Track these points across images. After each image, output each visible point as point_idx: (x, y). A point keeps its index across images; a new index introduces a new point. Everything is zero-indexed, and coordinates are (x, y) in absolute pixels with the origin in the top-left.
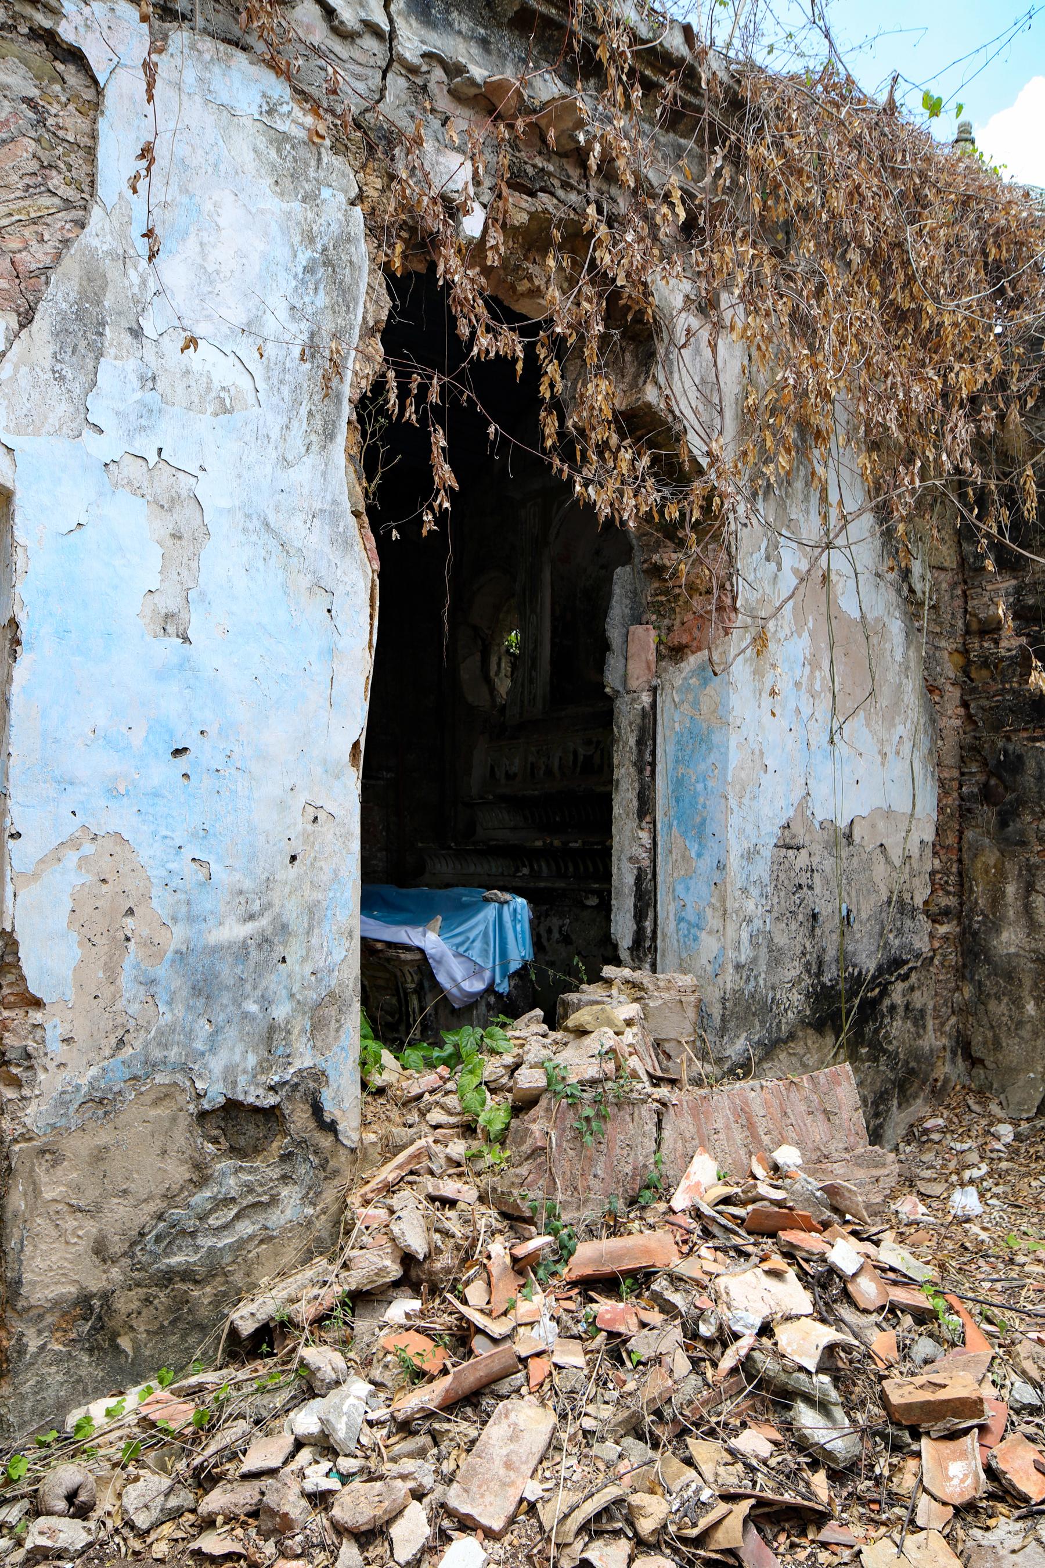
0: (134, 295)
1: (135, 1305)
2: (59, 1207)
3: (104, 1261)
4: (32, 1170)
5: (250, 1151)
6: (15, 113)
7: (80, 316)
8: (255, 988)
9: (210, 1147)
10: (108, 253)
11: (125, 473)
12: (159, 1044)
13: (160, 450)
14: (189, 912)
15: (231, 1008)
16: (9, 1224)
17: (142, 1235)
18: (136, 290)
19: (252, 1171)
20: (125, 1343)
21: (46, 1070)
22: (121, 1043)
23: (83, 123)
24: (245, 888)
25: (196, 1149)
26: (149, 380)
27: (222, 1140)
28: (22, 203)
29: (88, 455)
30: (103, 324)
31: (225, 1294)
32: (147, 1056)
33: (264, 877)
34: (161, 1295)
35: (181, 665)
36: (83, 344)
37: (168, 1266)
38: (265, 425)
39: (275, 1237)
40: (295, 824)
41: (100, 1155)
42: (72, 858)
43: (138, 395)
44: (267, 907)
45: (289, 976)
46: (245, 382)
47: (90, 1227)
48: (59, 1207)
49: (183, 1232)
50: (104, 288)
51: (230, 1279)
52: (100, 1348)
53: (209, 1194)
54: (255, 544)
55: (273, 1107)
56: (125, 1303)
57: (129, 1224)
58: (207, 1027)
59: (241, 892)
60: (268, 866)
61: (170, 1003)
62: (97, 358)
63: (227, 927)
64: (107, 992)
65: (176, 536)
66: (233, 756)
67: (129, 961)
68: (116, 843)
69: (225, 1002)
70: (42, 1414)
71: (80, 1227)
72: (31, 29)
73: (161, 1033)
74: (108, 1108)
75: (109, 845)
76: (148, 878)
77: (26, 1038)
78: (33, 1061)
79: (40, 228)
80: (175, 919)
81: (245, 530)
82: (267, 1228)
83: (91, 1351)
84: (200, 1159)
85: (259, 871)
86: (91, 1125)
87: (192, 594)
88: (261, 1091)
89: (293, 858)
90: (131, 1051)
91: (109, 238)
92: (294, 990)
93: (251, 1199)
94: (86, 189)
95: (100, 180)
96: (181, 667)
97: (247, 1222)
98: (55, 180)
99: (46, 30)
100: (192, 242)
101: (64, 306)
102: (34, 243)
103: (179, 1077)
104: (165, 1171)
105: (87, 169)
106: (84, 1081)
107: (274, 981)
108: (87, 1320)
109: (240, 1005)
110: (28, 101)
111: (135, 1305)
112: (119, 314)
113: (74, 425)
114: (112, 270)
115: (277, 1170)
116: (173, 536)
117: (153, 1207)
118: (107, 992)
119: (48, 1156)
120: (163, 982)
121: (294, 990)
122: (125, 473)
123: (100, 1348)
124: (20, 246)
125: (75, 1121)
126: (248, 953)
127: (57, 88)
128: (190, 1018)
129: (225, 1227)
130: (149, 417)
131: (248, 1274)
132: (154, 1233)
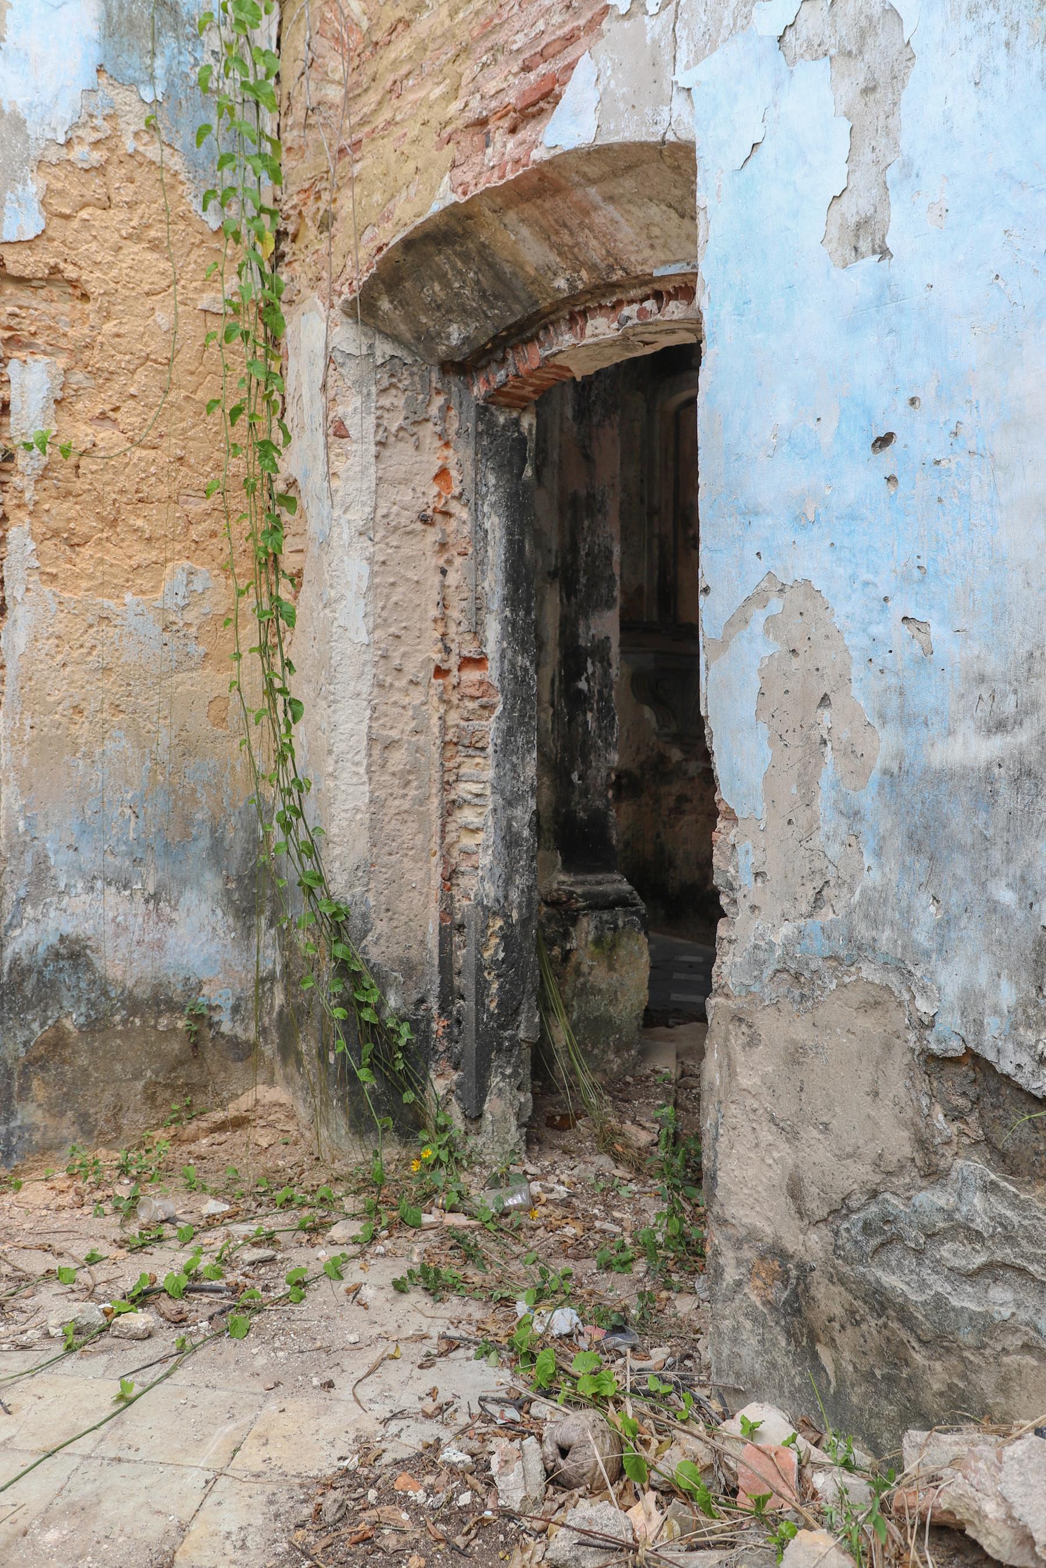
15: (969, 887)
19: (1015, 1203)
25: (919, 1111)
42: (759, 617)
53: (942, 1203)
58: (932, 909)
61: (879, 853)
64: (802, 817)
73: (867, 899)
74: (806, 991)
86: (786, 1006)
93: (1005, 1254)
109: (984, 885)
119: (744, 1028)
125: (769, 992)
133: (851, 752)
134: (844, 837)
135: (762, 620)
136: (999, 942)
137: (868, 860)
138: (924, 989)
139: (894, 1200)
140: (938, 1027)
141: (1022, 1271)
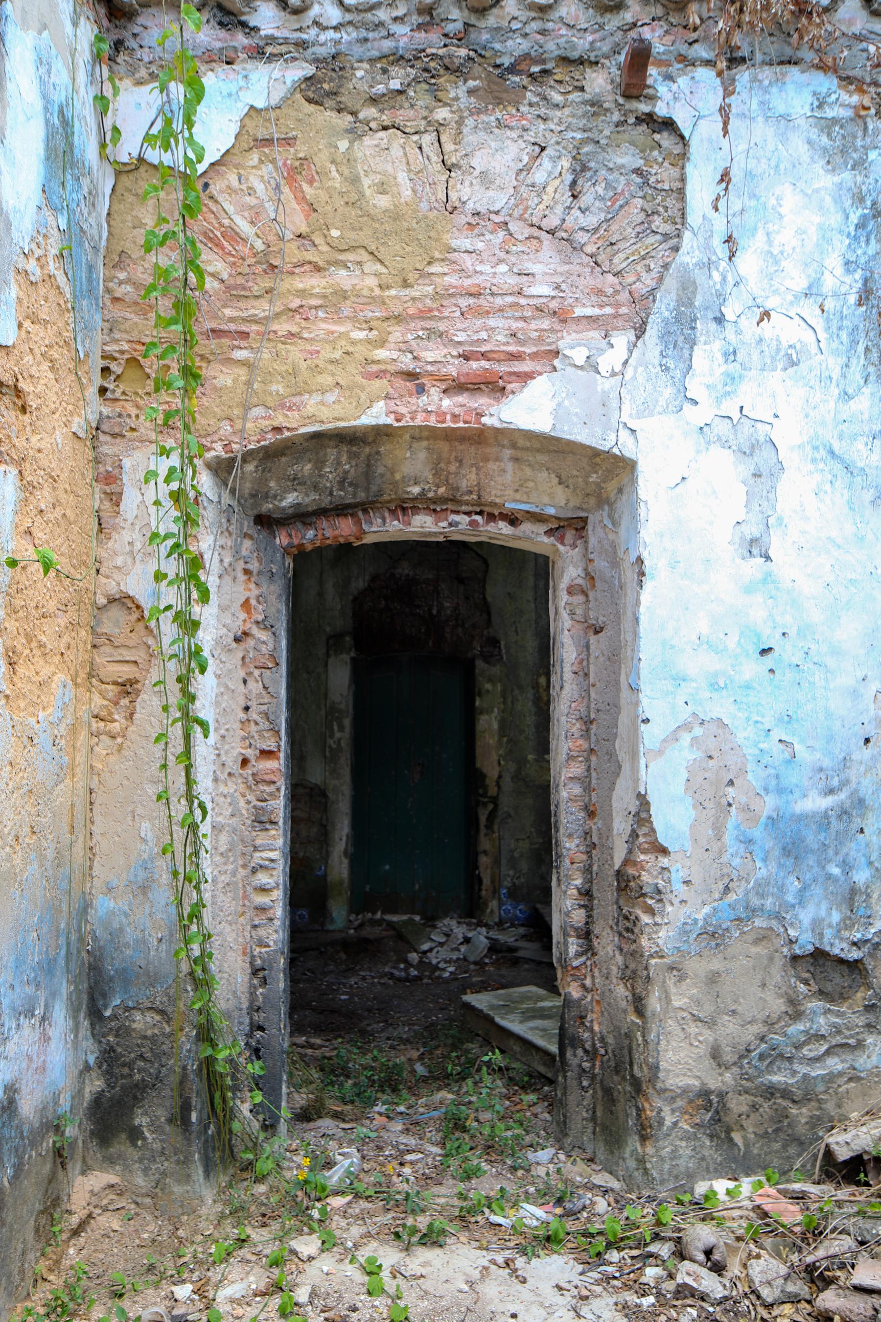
0: (717, 290)
1: (744, 1109)
2: (685, 1014)
3: (719, 1065)
4: (664, 982)
5: (836, 997)
6: (628, 184)
7: (677, 319)
8: (837, 854)
9: (802, 988)
10: (696, 264)
11: (716, 432)
12: (757, 894)
13: (742, 408)
14: (778, 784)
15: (816, 869)
16: (649, 1020)
17: (749, 1051)
18: (718, 287)
19: (839, 1014)
20: (737, 1137)
21: (672, 904)
22: (727, 889)
23: (674, 172)
24: (825, 765)
25: (790, 986)
26: (731, 355)
27: (812, 982)
28: (635, 247)
29: (688, 423)
30: (694, 320)
31: (819, 1118)
32: (748, 902)
33: (841, 757)
34: (766, 1105)
35: (765, 579)
36: (681, 338)
37: (770, 1082)
38: (827, 369)
39: (863, 1079)
40: (868, 711)
41: (713, 979)
42: (686, 738)
43: (724, 368)
44: (845, 783)
45: (867, 845)
46: (809, 337)
47: (708, 1035)
48: (685, 1014)
49: (781, 1056)
50: (694, 293)
51: (824, 1106)
52: (719, 1138)
53: (802, 1028)
54: (822, 470)
55: (856, 961)
56: (738, 1105)
57: (737, 1040)
58: (796, 883)
59: (821, 770)
60: (844, 748)
61: (765, 860)
62: (692, 347)
63: (810, 799)
65: (757, 475)
66: (810, 652)
67: (731, 823)
68: (718, 727)
69: (811, 863)
70: (676, 1177)
71: (700, 1034)
72: (637, 118)
73: (758, 884)
74: (719, 941)
75: (713, 728)
76: (744, 756)
77: (657, 877)
78: (663, 896)
79: (647, 262)
80: (766, 790)
81: (814, 460)
82: (854, 1069)
83: (711, 1137)
84: (794, 996)
85: (837, 751)
86: (706, 953)
87: (771, 521)
88: (845, 945)
89: (867, 741)
90: (735, 897)
91: (697, 252)
92: (872, 859)
93: (839, 1039)
94: (678, 220)
95: (688, 210)
96: (765, 581)
97: (836, 1060)
98: (657, 222)
99: (647, 114)
100: (761, 235)
101: (667, 314)
102: (644, 274)
103: (774, 924)
104: (765, 1001)
105: (679, 205)
106: (700, 916)
107: (853, 849)
108: (708, 1111)
109: (824, 868)
110: (638, 171)
111: (744, 1109)
112: (706, 309)
113: (677, 403)
114: (700, 277)
115: (862, 1018)
116: (754, 475)
117: (757, 1029)
118: (715, 847)
119: (675, 973)
120: (759, 842)
121: (872, 859)
122: (716, 432)
123: (719, 1138)
124: (634, 279)
125: (694, 948)
126: (829, 823)
127: (656, 153)
128: (782, 874)
129: (817, 1059)
130: (733, 384)
131: (839, 1106)
132: (758, 1051)
133: (746, 809)
134: (743, 854)
135: (689, 739)
136: (832, 893)
137: (759, 864)
138: (792, 924)
139: (776, 1037)
140: (800, 941)
141: (847, 1044)
